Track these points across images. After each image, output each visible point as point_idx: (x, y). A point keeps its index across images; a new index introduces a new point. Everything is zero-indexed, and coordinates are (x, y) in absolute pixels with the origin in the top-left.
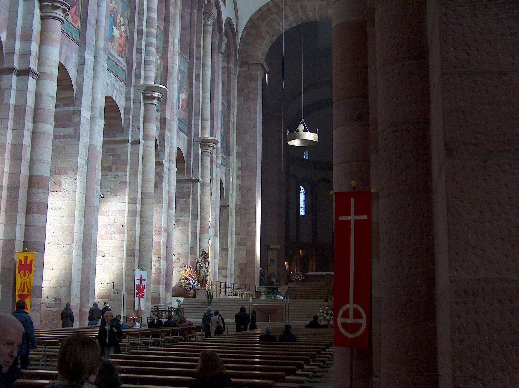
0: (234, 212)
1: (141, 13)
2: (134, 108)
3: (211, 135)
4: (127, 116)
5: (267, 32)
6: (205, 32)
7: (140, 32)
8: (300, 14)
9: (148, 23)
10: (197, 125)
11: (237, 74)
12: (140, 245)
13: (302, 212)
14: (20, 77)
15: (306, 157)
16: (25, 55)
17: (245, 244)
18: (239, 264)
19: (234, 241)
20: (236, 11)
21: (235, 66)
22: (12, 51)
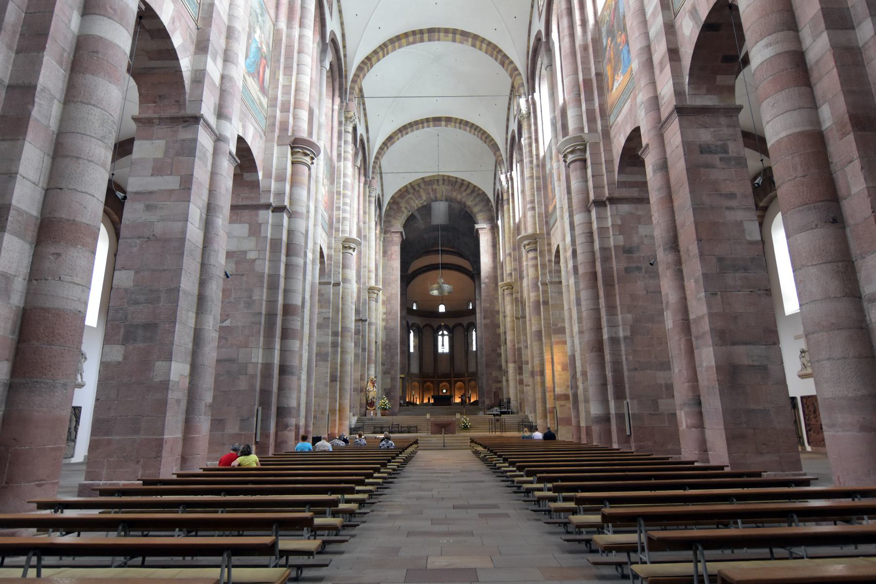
0: (380, 347)
1: (339, 178)
2: (335, 256)
3: (376, 282)
4: (329, 262)
6: (370, 202)
7: (339, 193)
8: (431, 195)
9: (344, 186)
10: (364, 276)
11: (382, 239)
12: (341, 372)
13: (412, 350)
14: (275, 214)
15: (415, 308)
16: (280, 194)
17: (389, 373)
18: (385, 389)
19: (380, 370)
20: (382, 190)
21: (381, 232)
22: (268, 189)
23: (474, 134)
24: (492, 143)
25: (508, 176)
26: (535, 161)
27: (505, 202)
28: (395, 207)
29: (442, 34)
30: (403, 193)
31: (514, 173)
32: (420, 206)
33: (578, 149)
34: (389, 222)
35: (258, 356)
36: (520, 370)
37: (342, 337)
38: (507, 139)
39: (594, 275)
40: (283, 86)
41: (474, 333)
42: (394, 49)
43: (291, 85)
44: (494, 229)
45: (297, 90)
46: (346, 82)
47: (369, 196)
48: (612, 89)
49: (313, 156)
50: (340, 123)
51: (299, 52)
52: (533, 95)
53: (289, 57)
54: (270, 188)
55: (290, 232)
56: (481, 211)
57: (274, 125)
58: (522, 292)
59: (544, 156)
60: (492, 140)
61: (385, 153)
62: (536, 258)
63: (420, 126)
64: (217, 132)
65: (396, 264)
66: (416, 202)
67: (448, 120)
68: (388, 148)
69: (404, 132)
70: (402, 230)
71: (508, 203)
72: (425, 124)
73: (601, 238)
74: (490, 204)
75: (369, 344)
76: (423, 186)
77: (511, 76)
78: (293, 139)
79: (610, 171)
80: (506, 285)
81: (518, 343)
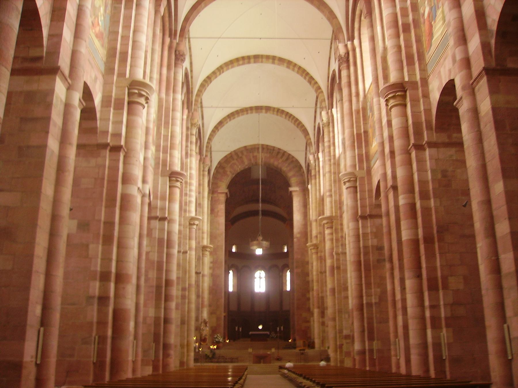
5: (230, 172)
6: (203, 175)
11: (210, 199)
15: (234, 250)
16: (163, 209)
23: (289, 120)
24: (303, 128)
25: (316, 157)
26: (332, 161)
27: (313, 177)
28: (221, 171)
29: (264, 60)
30: (228, 159)
31: (320, 155)
32: (242, 169)
33: (352, 180)
34: (216, 184)
35: (152, 312)
36: (322, 314)
37: (189, 292)
38: (315, 127)
39: (359, 262)
40: (164, 136)
41: (288, 274)
42: (228, 69)
43: (168, 135)
44: (305, 192)
45: (172, 136)
46: (192, 96)
47: (203, 171)
48: (372, 146)
49: (182, 181)
50: (187, 128)
51: (173, 110)
52: (332, 110)
53: (167, 116)
54: (157, 206)
55: (169, 233)
56: (294, 176)
57: (159, 164)
58: (325, 251)
59: (339, 157)
60: (303, 126)
61: (216, 134)
62: (332, 234)
63: (245, 113)
64: (143, 193)
65: (222, 220)
66: (240, 167)
67: (268, 109)
68: (218, 130)
69: (232, 118)
70: (226, 191)
71: (316, 179)
72: (249, 112)
73: (363, 240)
74: (302, 170)
75: (203, 292)
76: (245, 153)
77: (316, 91)
78: (170, 172)
79: (370, 197)
80: (312, 245)
81: (322, 292)
